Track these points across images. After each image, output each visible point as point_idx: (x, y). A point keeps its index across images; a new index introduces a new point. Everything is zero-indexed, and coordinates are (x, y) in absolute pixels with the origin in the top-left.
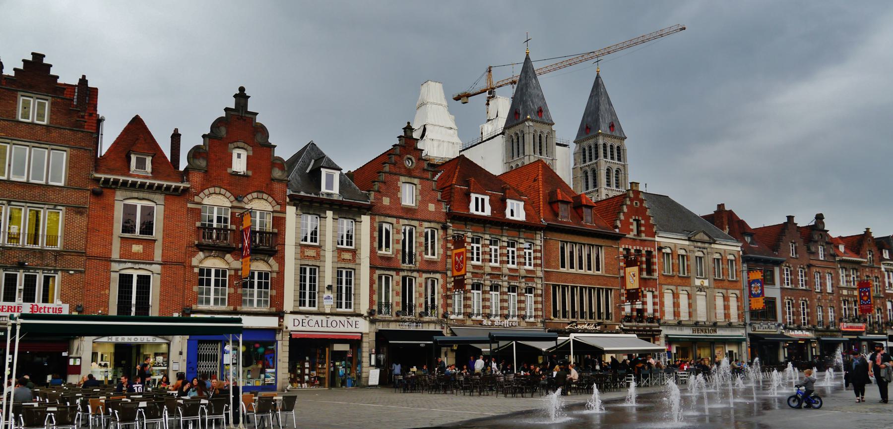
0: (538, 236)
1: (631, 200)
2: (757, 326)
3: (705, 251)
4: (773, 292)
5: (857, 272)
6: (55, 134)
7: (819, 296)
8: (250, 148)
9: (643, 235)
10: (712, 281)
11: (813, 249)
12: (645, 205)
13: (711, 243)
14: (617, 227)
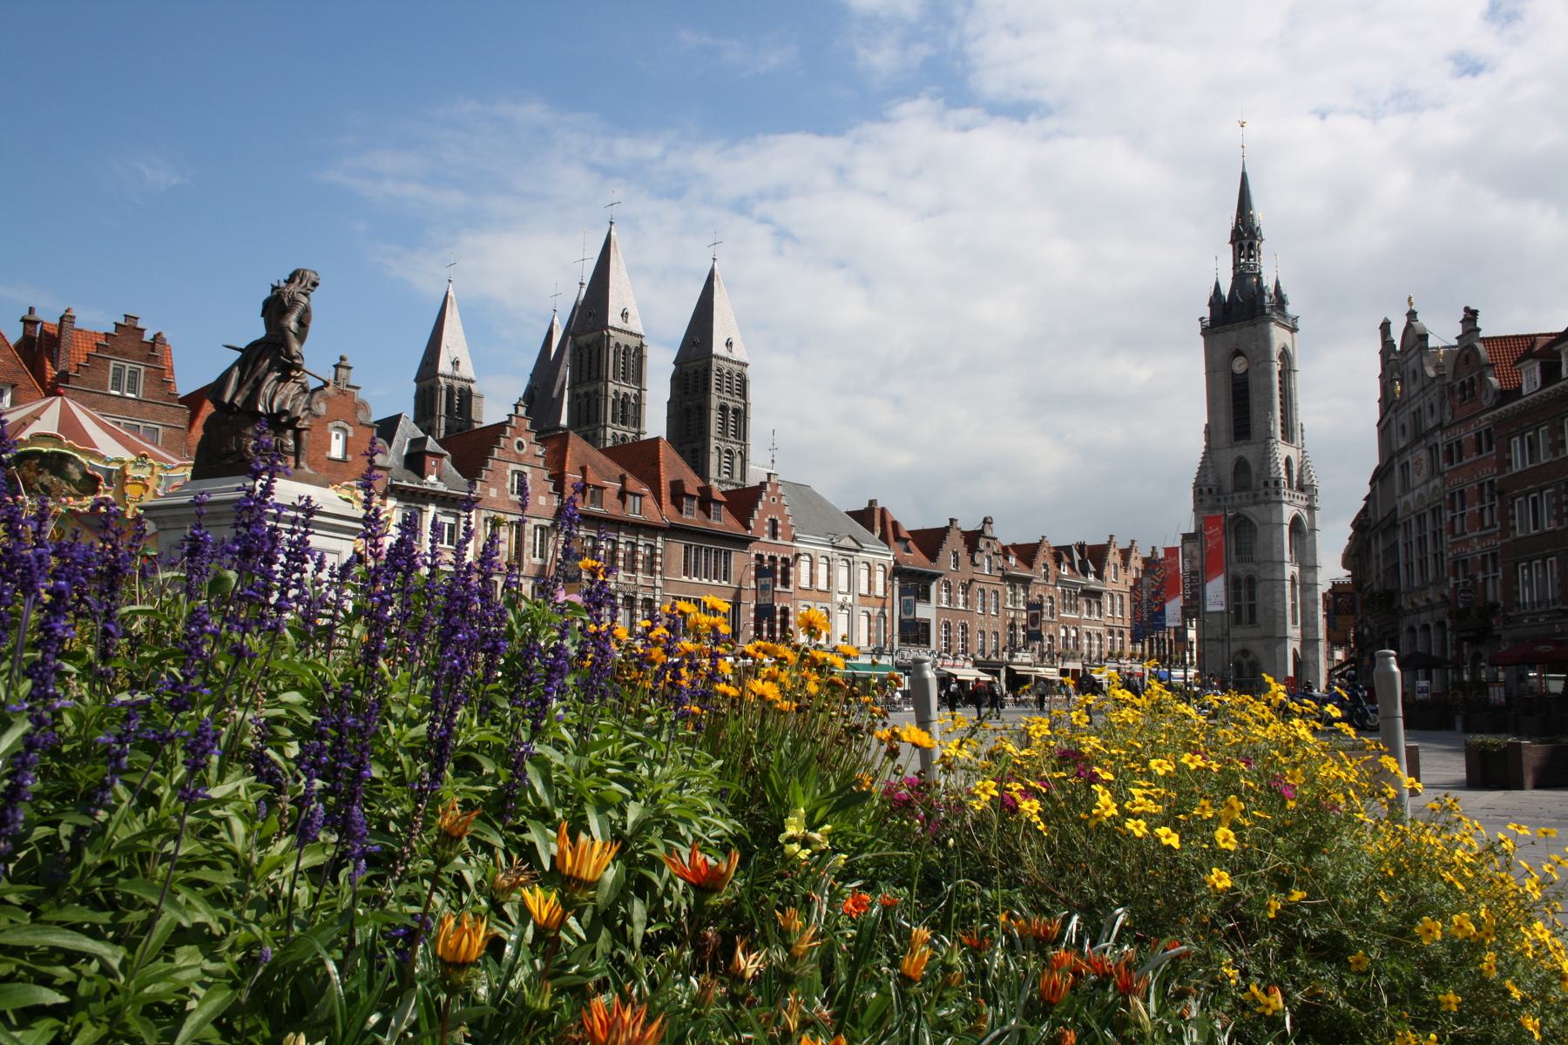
0: (659, 539)
1: (768, 496)
2: (906, 653)
3: (850, 559)
4: (923, 611)
5: (1026, 589)
6: (147, 408)
7: (982, 618)
8: (350, 429)
9: (779, 538)
10: (857, 596)
11: (978, 560)
12: (784, 501)
13: (857, 551)
14: (748, 528)
